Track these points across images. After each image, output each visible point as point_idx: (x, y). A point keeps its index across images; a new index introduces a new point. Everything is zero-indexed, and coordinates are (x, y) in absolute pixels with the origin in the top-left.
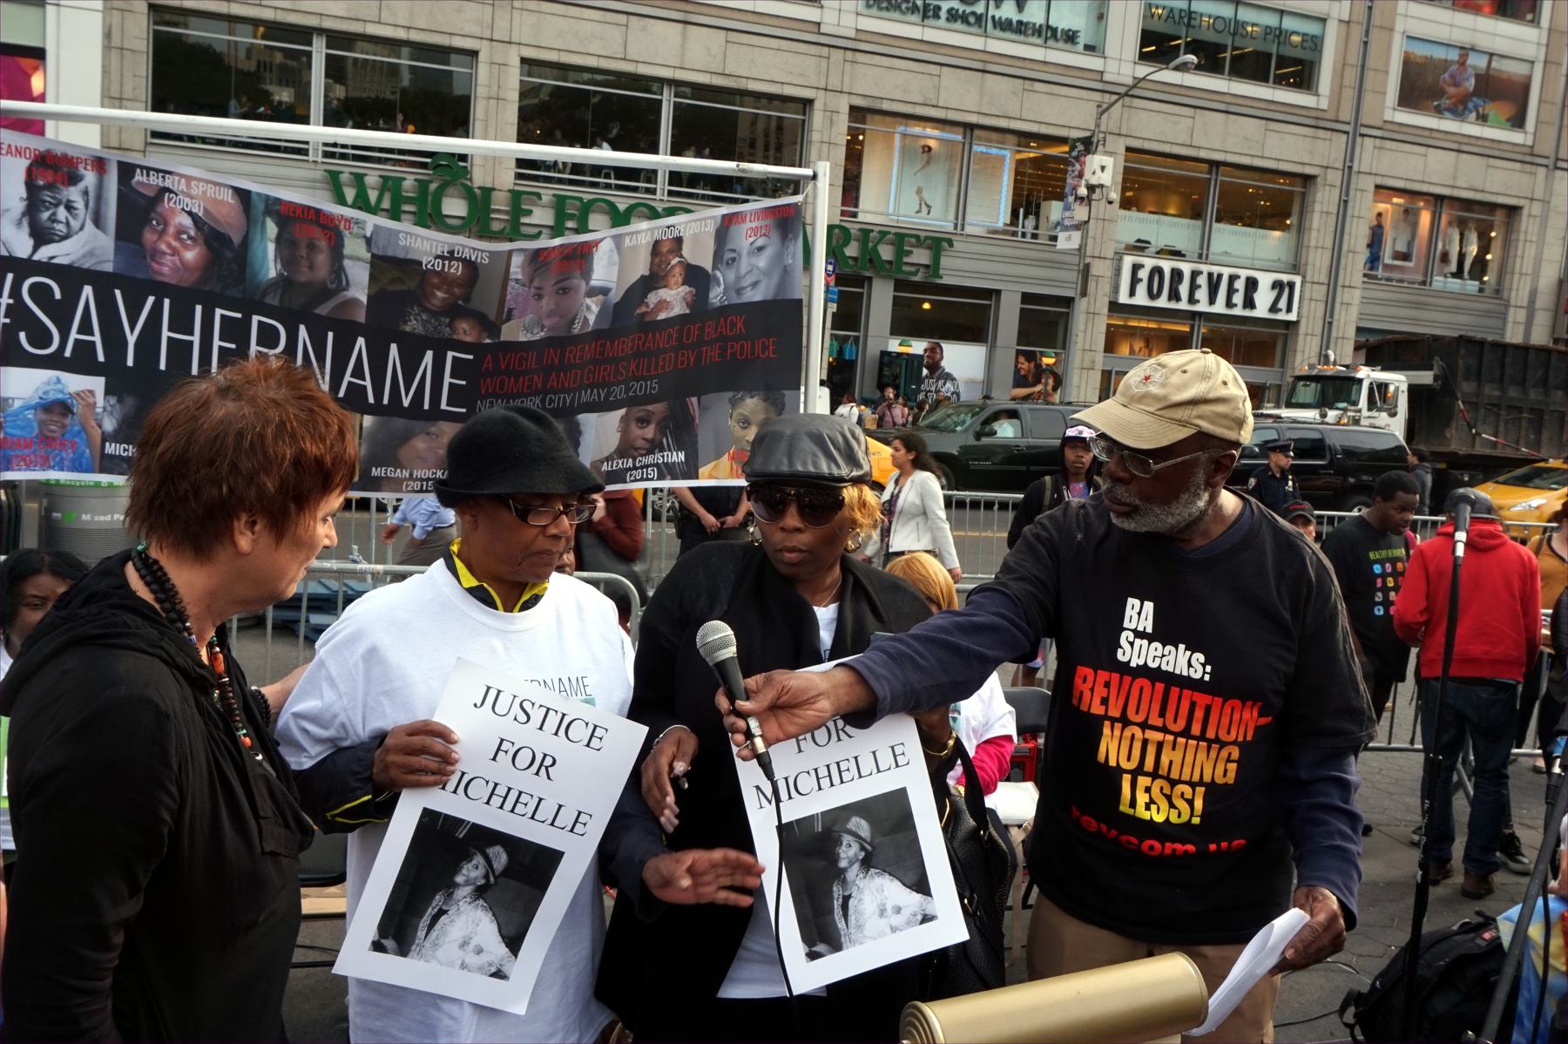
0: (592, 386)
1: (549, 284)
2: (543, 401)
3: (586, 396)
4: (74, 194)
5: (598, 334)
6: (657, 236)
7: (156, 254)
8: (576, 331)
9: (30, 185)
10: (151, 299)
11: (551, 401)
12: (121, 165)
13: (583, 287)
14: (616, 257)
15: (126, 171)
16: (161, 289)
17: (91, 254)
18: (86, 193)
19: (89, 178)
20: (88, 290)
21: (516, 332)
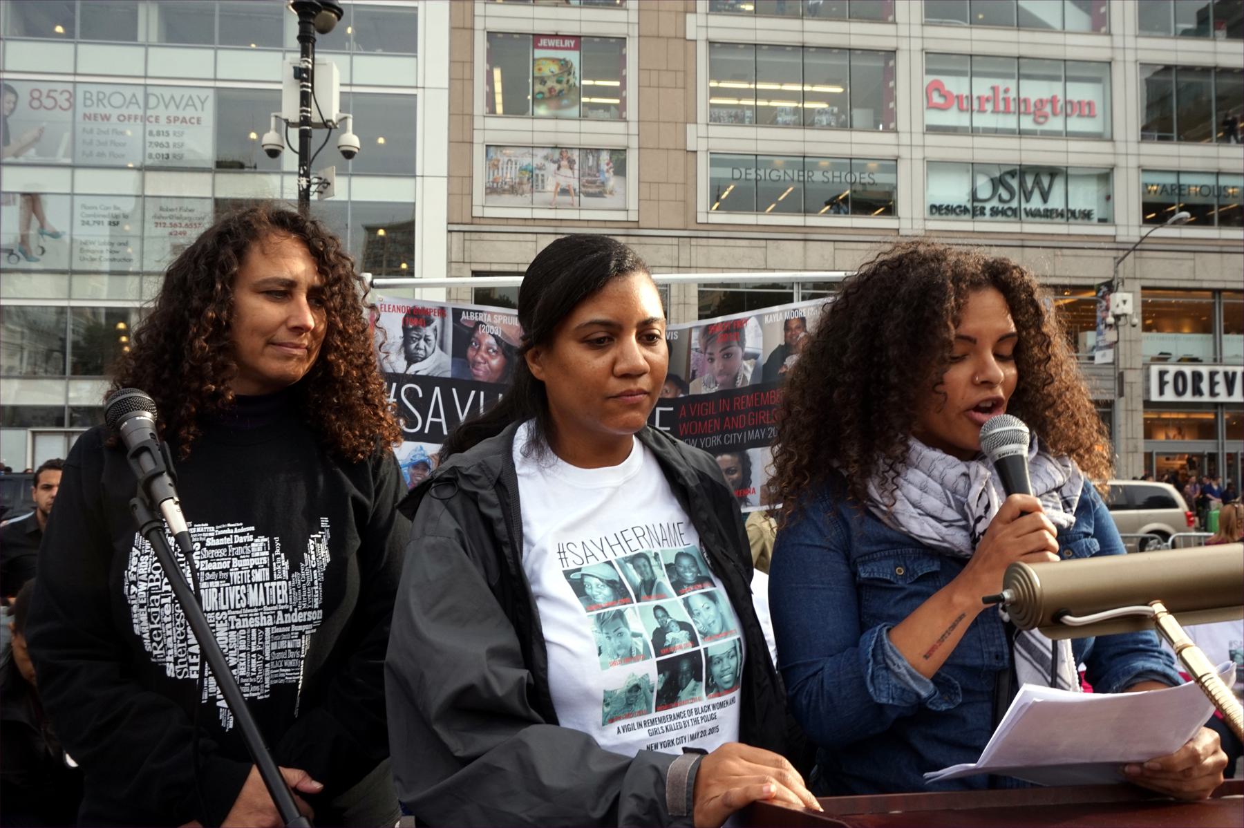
0: (755, 427)
1: (717, 355)
2: (722, 439)
3: (751, 435)
4: (428, 331)
5: (754, 388)
6: (787, 316)
7: (475, 363)
8: (739, 384)
9: (405, 329)
10: (473, 393)
11: (728, 439)
12: (454, 309)
13: (740, 354)
14: (760, 331)
15: (457, 313)
16: (478, 386)
17: (438, 367)
18: (435, 330)
19: (437, 322)
20: (437, 390)
21: (699, 387)
